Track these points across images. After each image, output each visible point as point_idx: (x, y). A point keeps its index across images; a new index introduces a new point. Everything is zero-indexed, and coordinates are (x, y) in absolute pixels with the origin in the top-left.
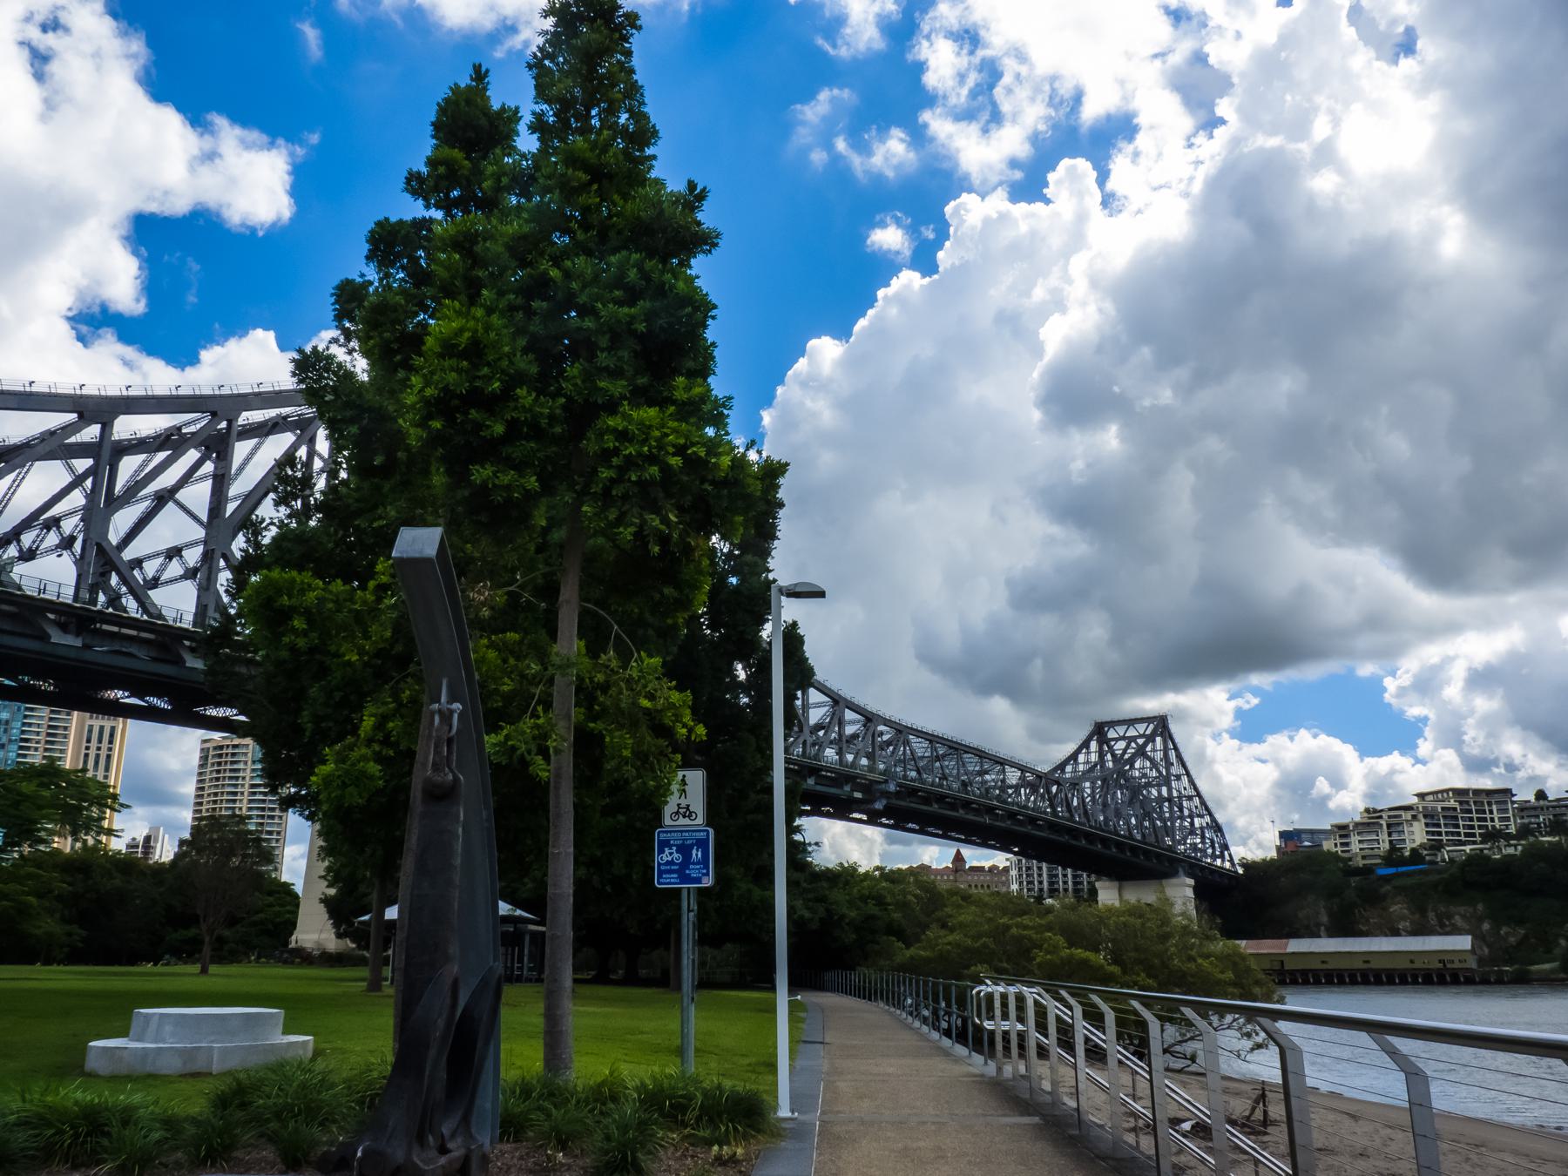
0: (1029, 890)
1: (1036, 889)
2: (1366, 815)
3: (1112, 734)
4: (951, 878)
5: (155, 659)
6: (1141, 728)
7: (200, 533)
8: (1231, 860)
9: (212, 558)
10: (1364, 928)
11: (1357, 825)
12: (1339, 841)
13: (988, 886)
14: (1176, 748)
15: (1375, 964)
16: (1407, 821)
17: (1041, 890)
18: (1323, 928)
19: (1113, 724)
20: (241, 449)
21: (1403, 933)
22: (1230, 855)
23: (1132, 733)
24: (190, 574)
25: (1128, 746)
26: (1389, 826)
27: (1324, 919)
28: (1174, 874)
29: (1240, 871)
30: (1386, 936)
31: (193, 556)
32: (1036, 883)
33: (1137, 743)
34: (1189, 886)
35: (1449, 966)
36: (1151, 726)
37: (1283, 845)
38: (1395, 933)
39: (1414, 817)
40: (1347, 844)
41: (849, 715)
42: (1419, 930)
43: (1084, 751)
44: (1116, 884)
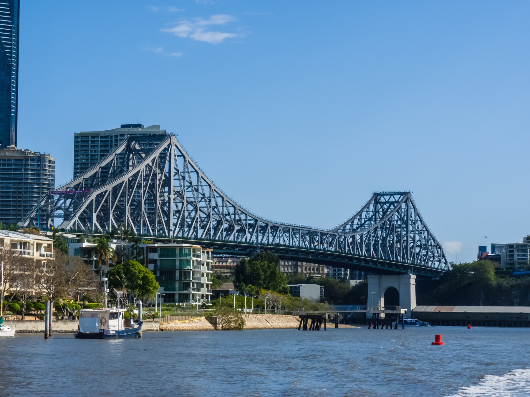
6: (397, 197)
8: (446, 263)
10: (498, 301)
11: (518, 245)
14: (414, 208)
19: (383, 194)
22: (446, 260)
23: (392, 200)
25: (390, 206)
29: (451, 269)
30: (508, 306)
33: (394, 206)
34: (413, 279)
36: (402, 197)
40: (513, 256)
44: (378, 276)
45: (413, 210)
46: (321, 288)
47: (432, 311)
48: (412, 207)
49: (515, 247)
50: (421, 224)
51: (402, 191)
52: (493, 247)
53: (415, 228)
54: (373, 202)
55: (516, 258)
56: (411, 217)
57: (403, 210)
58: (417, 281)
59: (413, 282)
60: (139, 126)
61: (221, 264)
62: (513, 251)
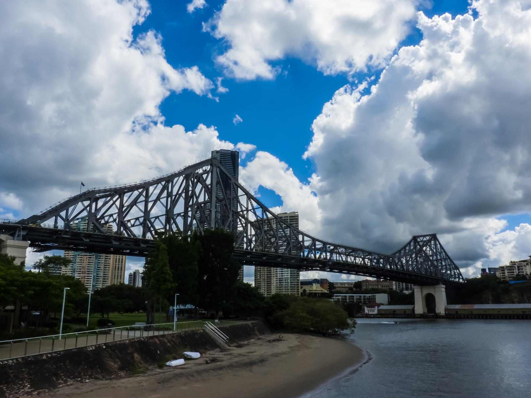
0: (399, 288)
1: (401, 288)
2: (511, 263)
3: (419, 240)
4: (376, 284)
5: (135, 245)
7: (142, 214)
8: (463, 278)
9: (145, 221)
10: (503, 301)
11: (507, 267)
12: (501, 272)
13: (389, 286)
14: (440, 244)
15: (502, 312)
16: (524, 265)
17: (403, 288)
18: (490, 301)
19: (419, 237)
20: (151, 189)
21: (516, 302)
22: (462, 277)
23: (425, 239)
24: (141, 224)
26: (518, 267)
27: (491, 298)
28: (438, 284)
30: (510, 303)
31: (141, 220)
32: (401, 285)
34: (443, 287)
35: (525, 313)
36: (431, 237)
37: (483, 273)
38: (513, 302)
39: (527, 264)
40: (504, 273)
41: (317, 243)
42: (520, 302)
43: (408, 246)
44: (420, 287)
45: (439, 245)
46: (388, 296)
47: (459, 308)
48: (438, 243)
49: (505, 268)
50: (445, 254)
51: (431, 234)
52: (490, 269)
53: (441, 257)
54: (413, 241)
55: (506, 274)
56: (438, 249)
57: (432, 246)
58: (446, 288)
59: (444, 290)
60: (286, 213)
61: (342, 286)
62: (504, 270)
